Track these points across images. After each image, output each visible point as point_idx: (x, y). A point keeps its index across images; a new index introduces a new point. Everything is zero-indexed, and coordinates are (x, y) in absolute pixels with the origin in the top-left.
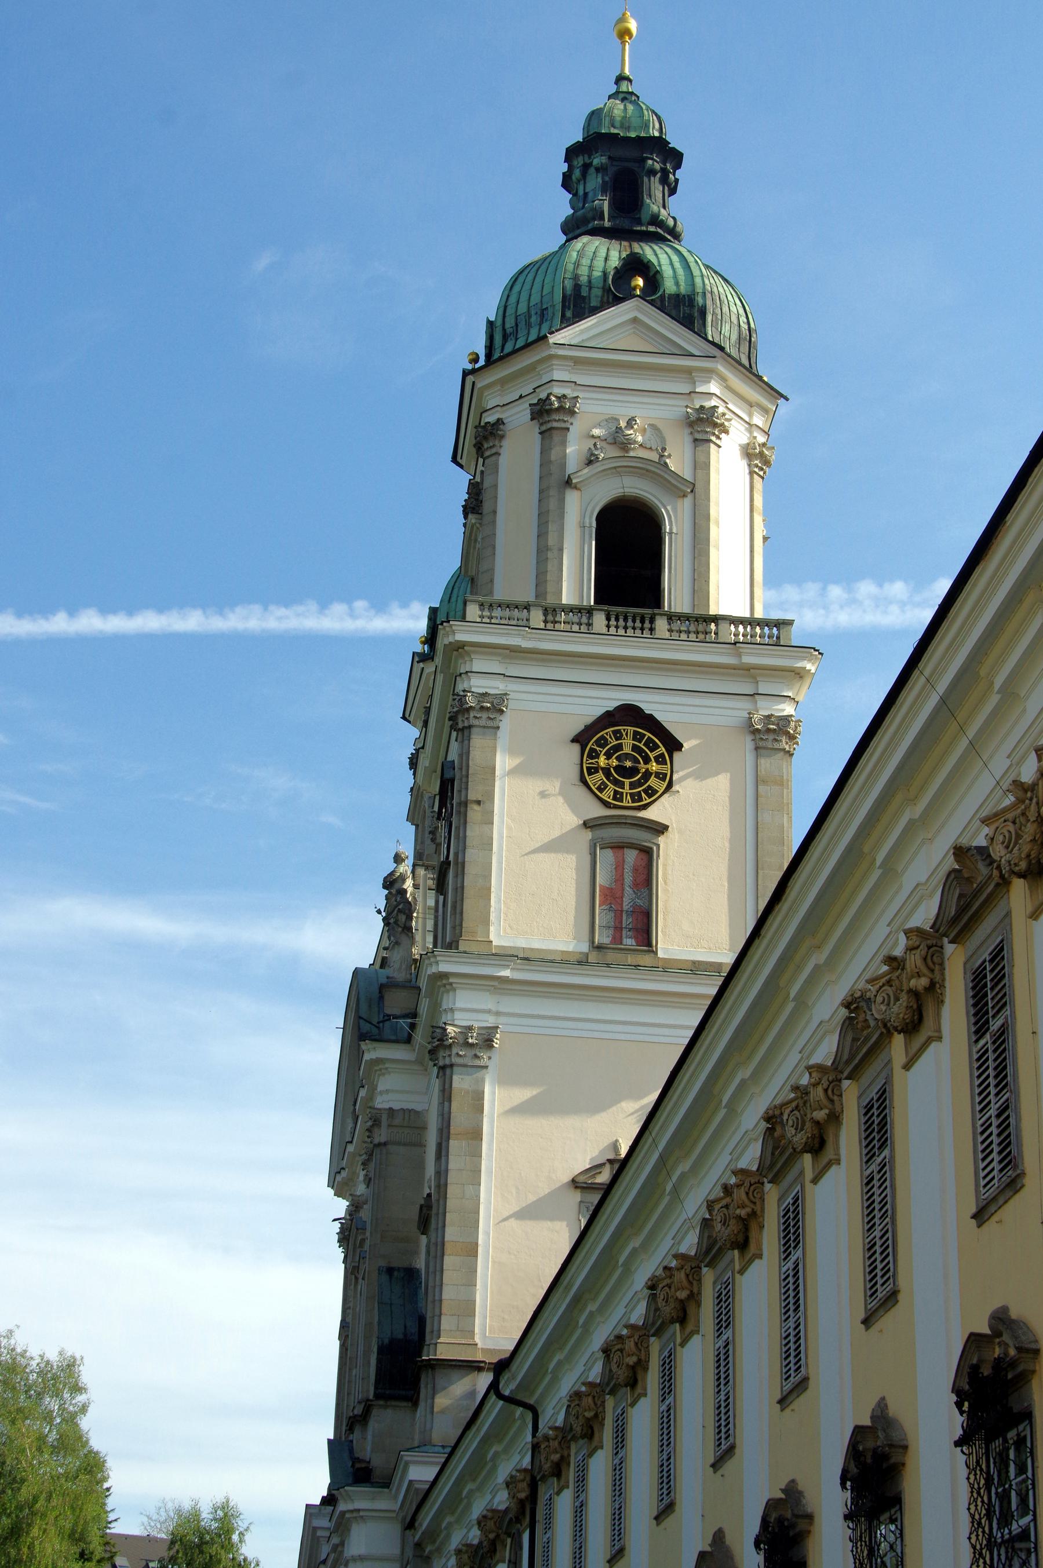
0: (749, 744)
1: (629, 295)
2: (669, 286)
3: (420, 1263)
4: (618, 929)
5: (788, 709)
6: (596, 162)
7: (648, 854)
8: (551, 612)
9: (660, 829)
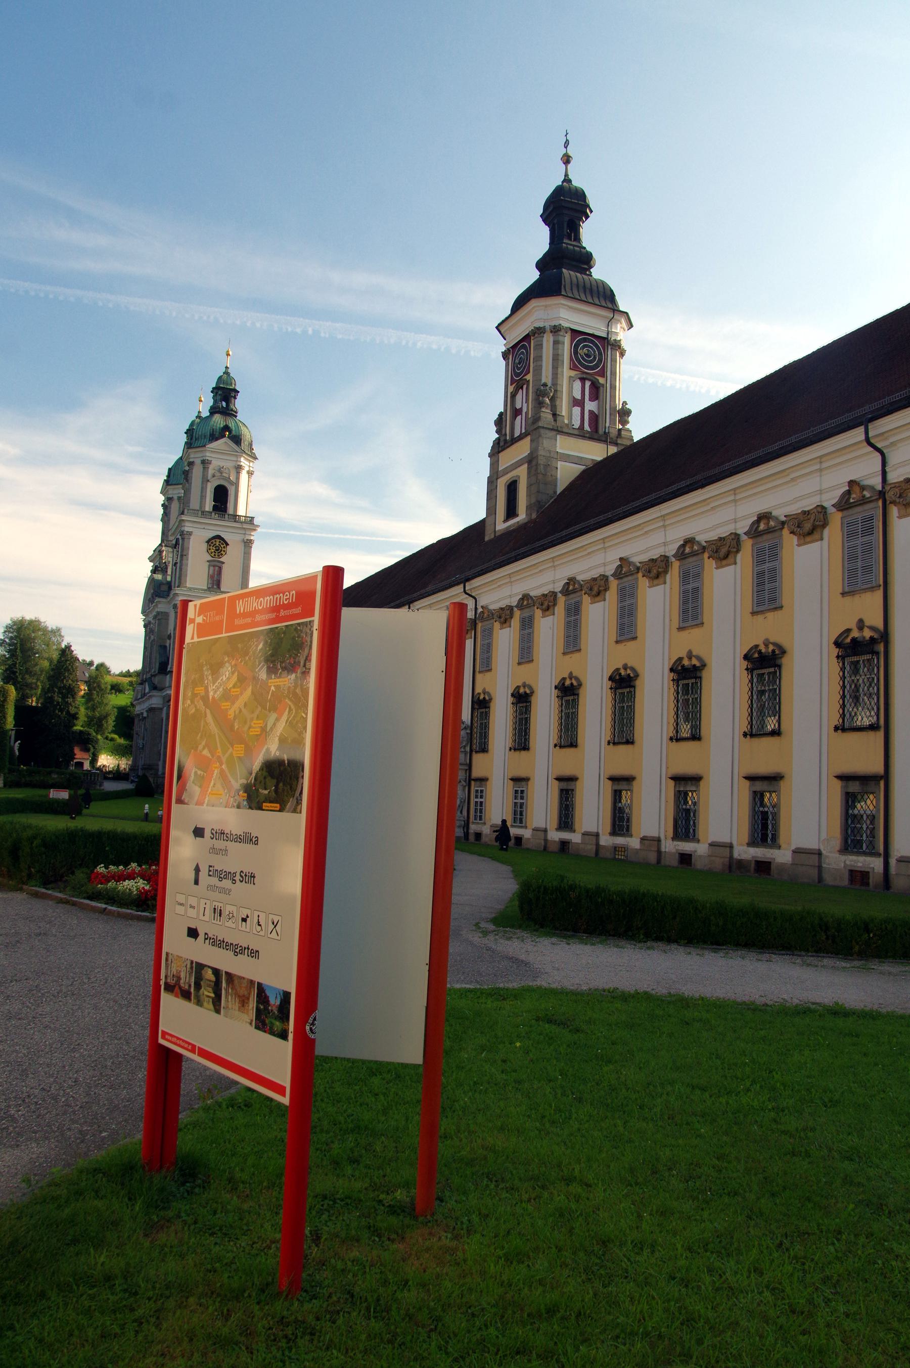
0: (243, 544)
2: (234, 433)
3: (168, 645)
5: (252, 538)
7: (220, 568)
8: (203, 512)
9: (223, 563)
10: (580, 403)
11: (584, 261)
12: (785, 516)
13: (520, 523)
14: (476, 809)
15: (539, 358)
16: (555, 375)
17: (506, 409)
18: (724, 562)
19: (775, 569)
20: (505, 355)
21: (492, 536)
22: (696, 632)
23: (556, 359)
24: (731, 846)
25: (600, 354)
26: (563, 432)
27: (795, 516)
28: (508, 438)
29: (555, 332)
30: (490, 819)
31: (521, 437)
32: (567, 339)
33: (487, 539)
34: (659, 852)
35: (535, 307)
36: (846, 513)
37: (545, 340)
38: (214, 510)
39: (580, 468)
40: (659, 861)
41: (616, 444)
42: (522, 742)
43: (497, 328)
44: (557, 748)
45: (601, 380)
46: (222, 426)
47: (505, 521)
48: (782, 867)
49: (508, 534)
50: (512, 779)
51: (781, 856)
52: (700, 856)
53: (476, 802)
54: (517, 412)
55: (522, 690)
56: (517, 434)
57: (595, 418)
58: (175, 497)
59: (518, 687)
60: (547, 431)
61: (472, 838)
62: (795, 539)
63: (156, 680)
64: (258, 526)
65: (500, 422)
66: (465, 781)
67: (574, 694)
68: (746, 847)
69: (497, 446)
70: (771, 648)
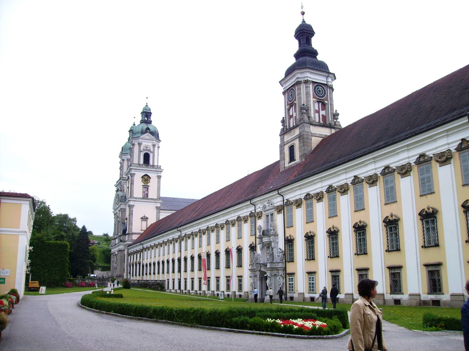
0: (157, 178)
1: (147, 132)
4: (145, 195)
6: (144, 114)
7: (148, 188)
8: (139, 164)
9: (149, 186)
10: (318, 112)
11: (314, 53)
12: (433, 155)
13: (297, 163)
14: (290, 287)
15: (300, 94)
16: (308, 101)
17: (286, 116)
18: (405, 176)
19: (429, 177)
20: (284, 93)
21: (284, 169)
22: (394, 205)
23: (307, 94)
24: (419, 295)
25: (325, 91)
26: (312, 124)
27: (437, 155)
28: (288, 128)
29: (306, 83)
30: (297, 291)
31: (294, 127)
32: (311, 86)
33: (281, 170)
34: (384, 300)
35: (297, 73)
36: (461, 152)
37: (302, 86)
38: (144, 163)
39: (321, 139)
40: (384, 303)
41: (334, 128)
42: (311, 256)
43: (280, 82)
44: (329, 258)
45: (326, 102)
46: (146, 128)
47: (289, 163)
48: (445, 303)
49: (291, 168)
50: (307, 273)
51: (445, 297)
52: (404, 300)
53: (290, 284)
54: (291, 117)
55: (309, 234)
56: (291, 126)
57: (324, 117)
58: (125, 159)
59: (307, 233)
60: (306, 124)
61: (288, 299)
62: (438, 164)
63: (122, 238)
64: (163, 170)
65: (283, 121)
66: (284, 275)
67: (336, 235)
68: (427, 295)
69: (282, 131)
70: (431, 210)
